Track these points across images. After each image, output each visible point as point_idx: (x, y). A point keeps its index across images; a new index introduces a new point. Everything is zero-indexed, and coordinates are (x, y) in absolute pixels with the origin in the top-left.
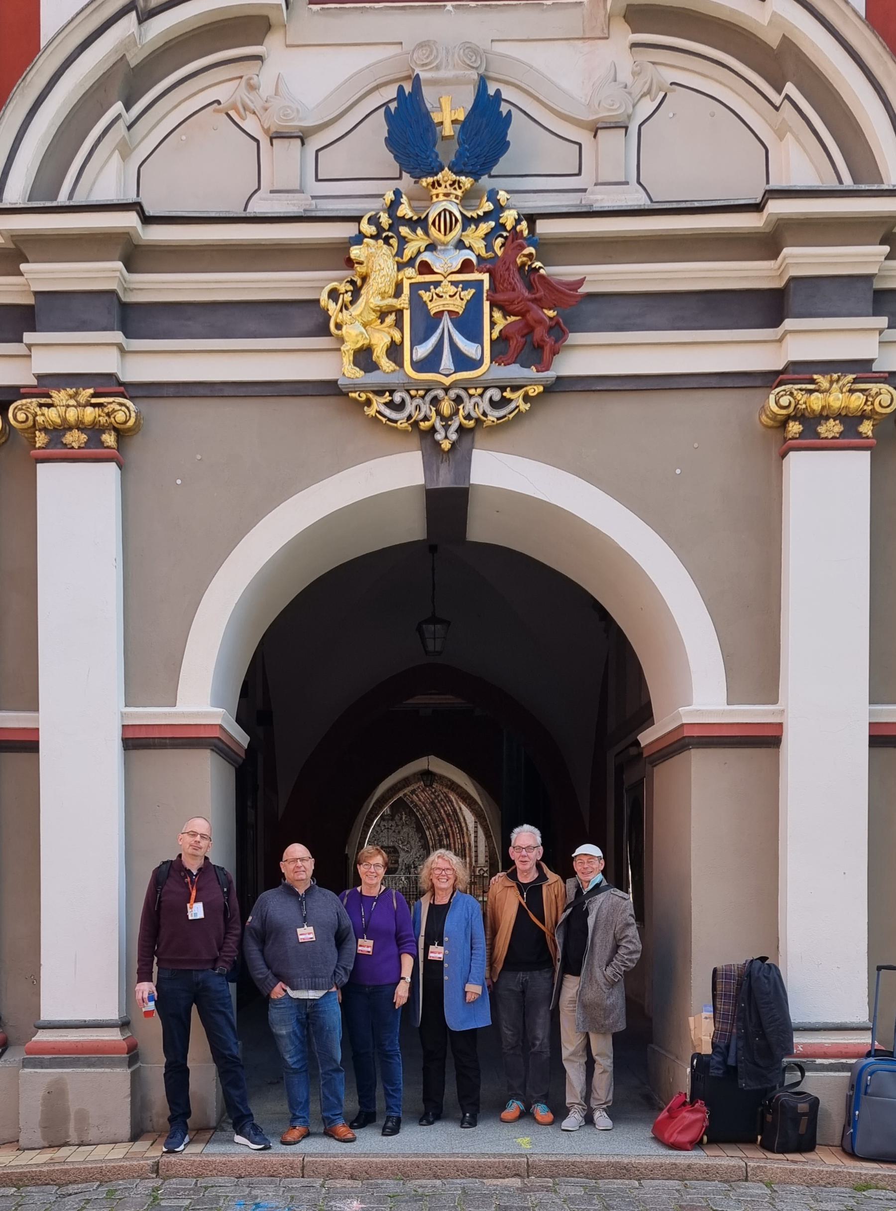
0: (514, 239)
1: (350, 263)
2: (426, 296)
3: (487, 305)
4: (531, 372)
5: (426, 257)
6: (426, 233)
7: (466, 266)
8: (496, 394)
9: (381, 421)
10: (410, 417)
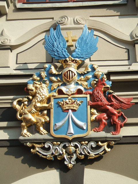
0: (100, 82)
4: (109, 135)
6: (61, 79)
7: (79, 92)
9: (39, 156)
10: (53, 154)
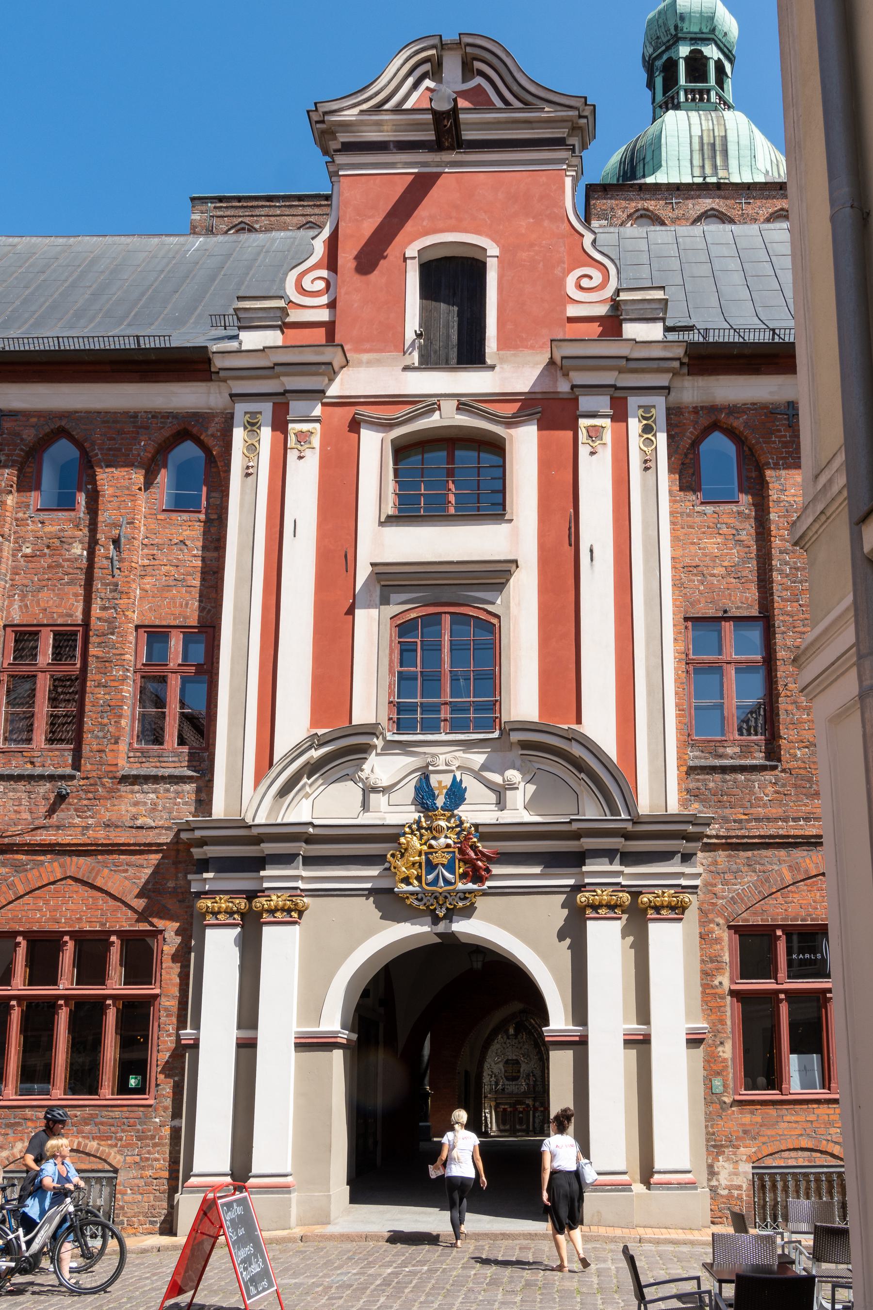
1: (400, 844)
4: (475, 887)
5: (433, 842)
8: (462, 895)
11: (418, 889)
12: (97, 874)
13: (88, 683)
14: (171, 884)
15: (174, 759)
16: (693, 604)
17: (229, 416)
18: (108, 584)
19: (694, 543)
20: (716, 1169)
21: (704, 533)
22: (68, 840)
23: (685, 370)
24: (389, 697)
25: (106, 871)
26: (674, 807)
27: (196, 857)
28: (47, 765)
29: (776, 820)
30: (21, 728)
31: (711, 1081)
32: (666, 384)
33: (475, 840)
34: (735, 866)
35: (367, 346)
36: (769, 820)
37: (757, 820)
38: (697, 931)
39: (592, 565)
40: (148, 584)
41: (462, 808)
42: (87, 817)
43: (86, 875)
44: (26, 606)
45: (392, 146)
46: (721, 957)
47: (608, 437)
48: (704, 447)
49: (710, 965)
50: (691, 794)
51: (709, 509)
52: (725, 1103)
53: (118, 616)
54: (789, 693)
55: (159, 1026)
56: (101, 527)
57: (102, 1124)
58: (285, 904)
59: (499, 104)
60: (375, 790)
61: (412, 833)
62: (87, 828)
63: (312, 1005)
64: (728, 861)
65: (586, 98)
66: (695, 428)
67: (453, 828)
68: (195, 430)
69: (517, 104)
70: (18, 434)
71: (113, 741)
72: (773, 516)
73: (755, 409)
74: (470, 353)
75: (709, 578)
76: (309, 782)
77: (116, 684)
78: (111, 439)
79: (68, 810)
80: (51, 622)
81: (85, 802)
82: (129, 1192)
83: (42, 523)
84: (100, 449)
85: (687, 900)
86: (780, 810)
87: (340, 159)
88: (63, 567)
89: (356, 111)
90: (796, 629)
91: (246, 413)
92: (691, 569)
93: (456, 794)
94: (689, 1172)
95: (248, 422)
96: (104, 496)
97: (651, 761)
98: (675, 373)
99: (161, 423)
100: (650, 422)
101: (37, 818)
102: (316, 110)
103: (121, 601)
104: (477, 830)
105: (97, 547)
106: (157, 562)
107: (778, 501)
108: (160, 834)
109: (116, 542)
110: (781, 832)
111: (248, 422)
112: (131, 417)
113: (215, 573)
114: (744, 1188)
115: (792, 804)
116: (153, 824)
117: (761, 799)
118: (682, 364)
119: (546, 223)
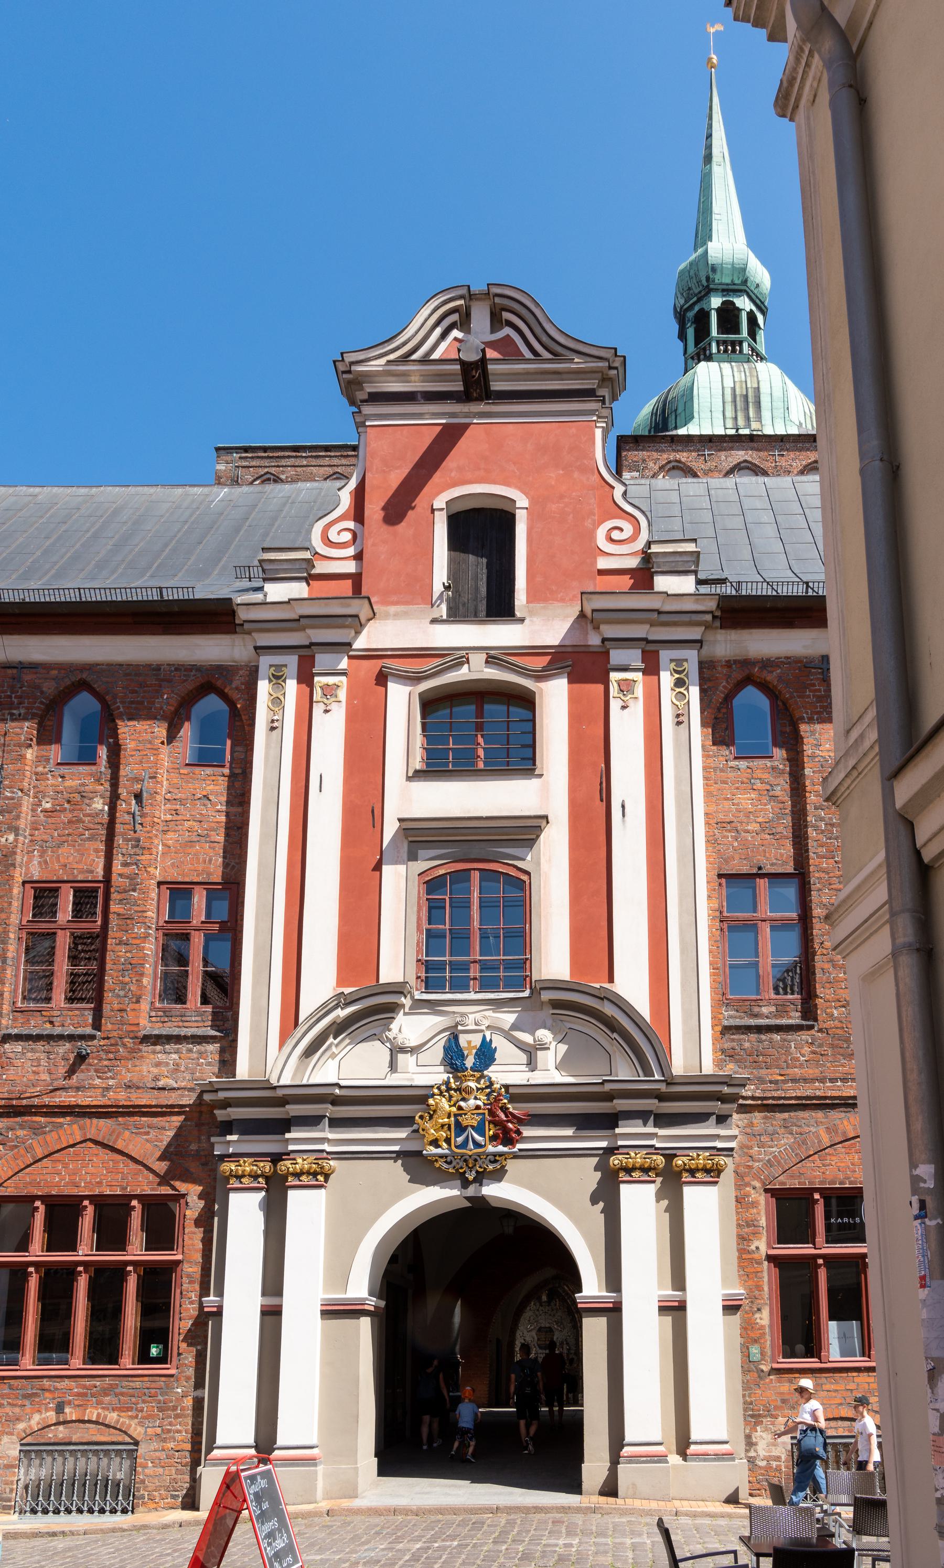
1: (428, 1105)
2: (460, 1119)
3: (487, 1123)
4: (506, 1149)
5: (462, 1104)
8: (492, 1158)
11: (447, 1151)
12: (118, 1137)
13: (109, 941)
14: (194, 1147)
15: (197, 1018)
16: (727, 861)
17: (254, 669)
18: (130, 840)
19: (728, 799)
20: (754, 1440)
21: (737, 788)
22: (88, 1101)
23: (718, 623)
24: (417, 956)
25: (127, 1133)
26: (708, 1067)
27: (219, 1119)
28: (66, 1024)
29: (813, 1080)
30: (39, 987)
31: (748, 1348)
32: (699, 638)
33: (506, 1101)
34: (771, 1128)
35: (394, 598)
36: (805, 1080)
37: (794, 1081)
38: (732, 1194)
39: (624, 821)
40: (171, 839)
41: (492, 1068)
42: (107, 1078)
43: (107, 1137)
44: (46, 862)
45: (419, 396)
46: (758, 1221)
47: (639, 690)
48: (737, 701)
49: (746, 1230)
50: (726, 1055)
51: (743, 764)
52: (762, 1371)
53: (140, 873)
54: (825, 952)
55: (181, 1293)
56: (123, 781)
57: (122, 1394)
58: (311, 1168)
59: (528, 354)
60: (403, 1050)
61: (441, 1094)
62: (107, 1089)
63: (339, 1271)
64: (764, 1123)
65: (616, 349)
66: (727, 682)
67: (482, 1089)
68: (219, 683)
69: (546, 355)
70: (38, 687)
71: (134, 1000)
72: (807, 771)
73: (789, 663)
74: (500, 607)
75: (743, 834)
76: (336, 1042)
77: (137, 942)
78: (133, 692)
79: (88, 1070)
80: (71, 878)
81: (106, 1063)
82: (150, 1465)
83: (63, 777)
84: (122, 702)
85: (722, 1163)
86: (816, 1071)
87: (367, 410)
88: (84, 822)
89: (383, 361)
90: (832, 886)
91: (271, 666)
92: (725, 825)
93: (486, 1055)
94: (726, 1442)
95: (273, 675)
96: (126, 750)
97: (685, 1021)
98: (708, 626)
99: (184, 675)
100: (682, 676)
101: (56, 1079)
102: (343, 360)
103: (143, 857)
104: (507, 1092)
105: (118, 802)
106: (179, 818)
107: (813, 756)
108: (183, 1096)
109: (138, 797)
110: (818, 1093)
111: (273, 675)
112: (154, 670)
113: (239, 828)
114: (783, 1459)
115: (829, 1064)
116: (175, 1085)
117: (797, 1059)
118: (714, 617)
119: (576, 475)
